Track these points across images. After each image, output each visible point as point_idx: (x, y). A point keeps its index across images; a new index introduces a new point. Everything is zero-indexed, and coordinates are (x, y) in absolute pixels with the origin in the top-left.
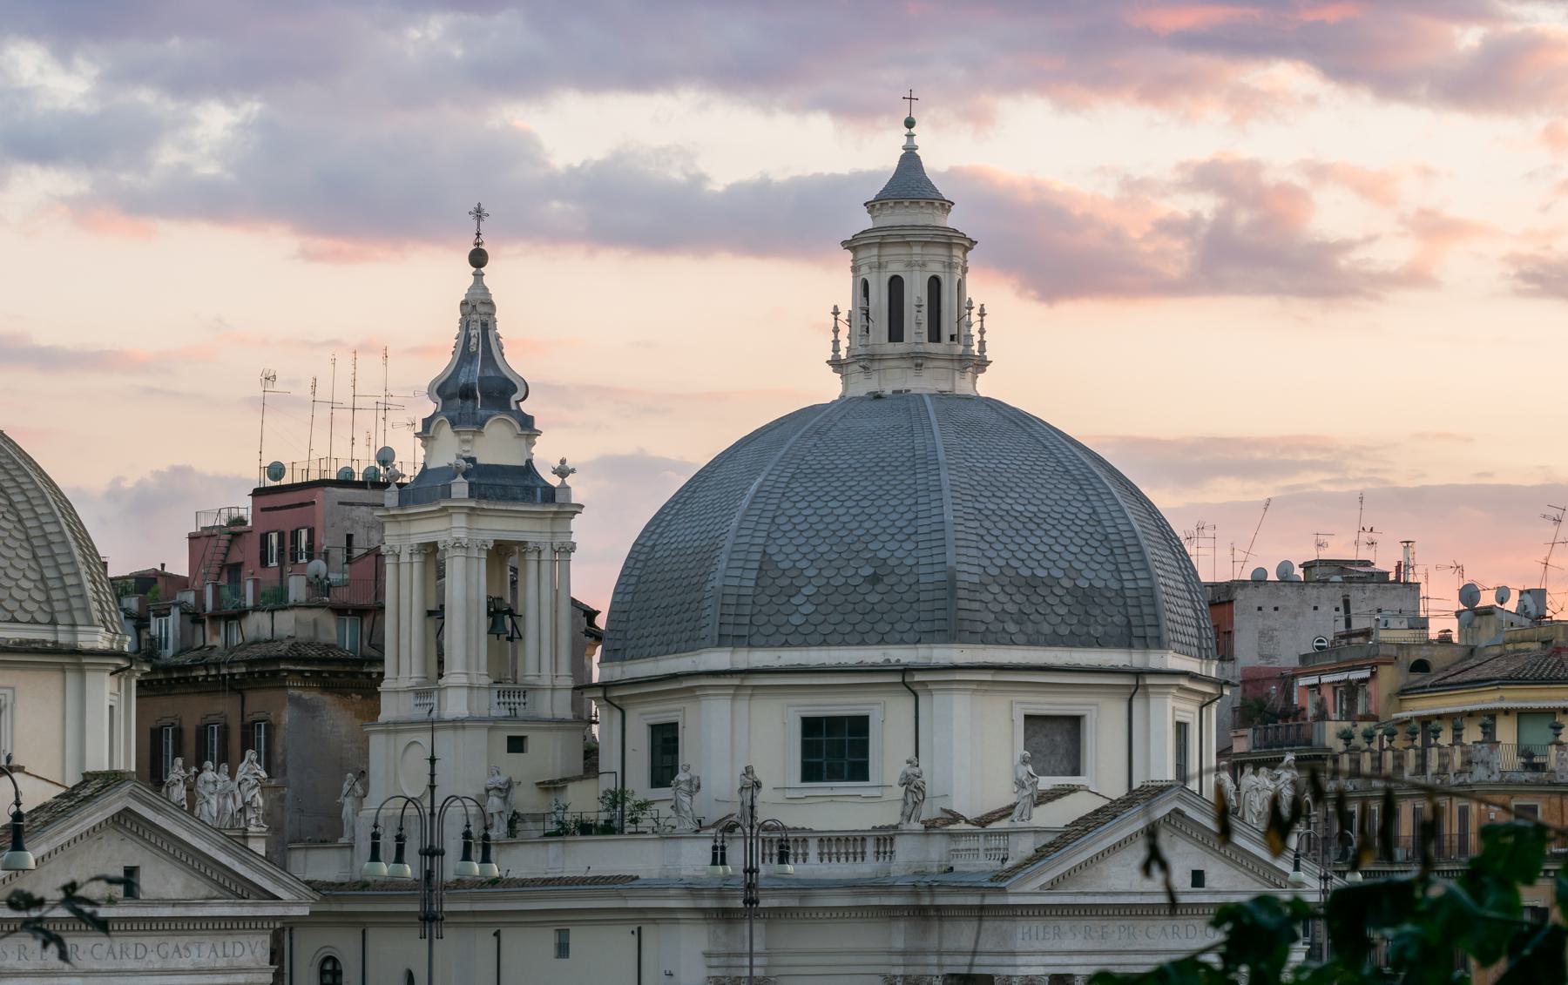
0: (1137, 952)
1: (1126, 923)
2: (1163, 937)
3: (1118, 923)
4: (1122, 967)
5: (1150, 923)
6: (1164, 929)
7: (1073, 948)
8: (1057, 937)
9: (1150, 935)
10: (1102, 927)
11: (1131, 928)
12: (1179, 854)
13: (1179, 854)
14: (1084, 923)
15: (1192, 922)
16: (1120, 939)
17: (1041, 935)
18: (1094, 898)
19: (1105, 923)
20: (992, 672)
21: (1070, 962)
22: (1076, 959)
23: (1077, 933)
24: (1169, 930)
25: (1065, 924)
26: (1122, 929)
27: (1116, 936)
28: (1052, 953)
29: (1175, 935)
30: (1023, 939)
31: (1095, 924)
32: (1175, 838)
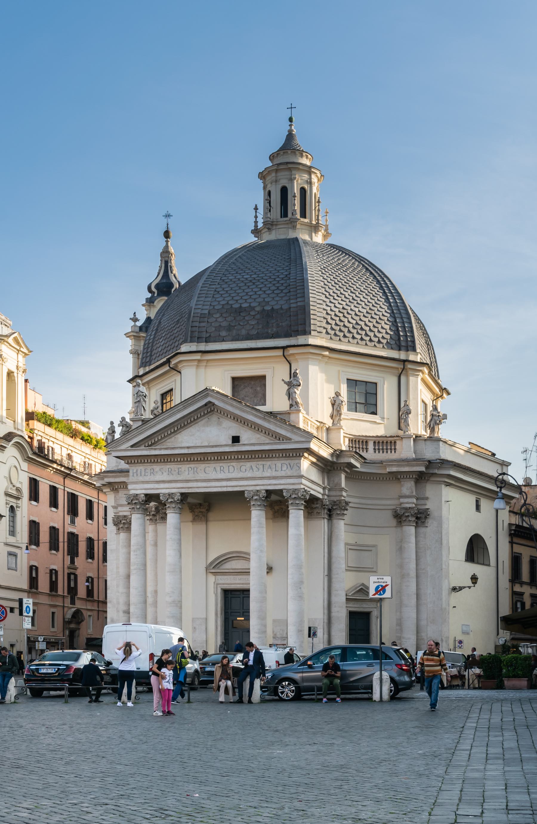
0: (197, 481)
1: (192, 466)
2: (214, 472)
3: (188, 466)
4: (190, 489)
5: (207, 465)
6: (215, 468)
7: (161, 479)
8: (152, 474)
9: (207, 472)
10: (178, 468)
11: (195, 469)
12: (224, 428)
13: (224, 428)
14: (168, 466)
15: (232, 464)
16: (188, 474)
17: (143, 473)
18: (160, 451)
19: (180, 466)
20: (200, 354)
21: (159, 487)
22: (162, 485)
23: (164, 472)
24: (218, 469)
25: (157, 467)
26: (190, 469)
27: (187, 473)
28: (147, 482)
29: (222, 471)
30: (133, 476)
31: (173, 467)
32: (221, 420)
